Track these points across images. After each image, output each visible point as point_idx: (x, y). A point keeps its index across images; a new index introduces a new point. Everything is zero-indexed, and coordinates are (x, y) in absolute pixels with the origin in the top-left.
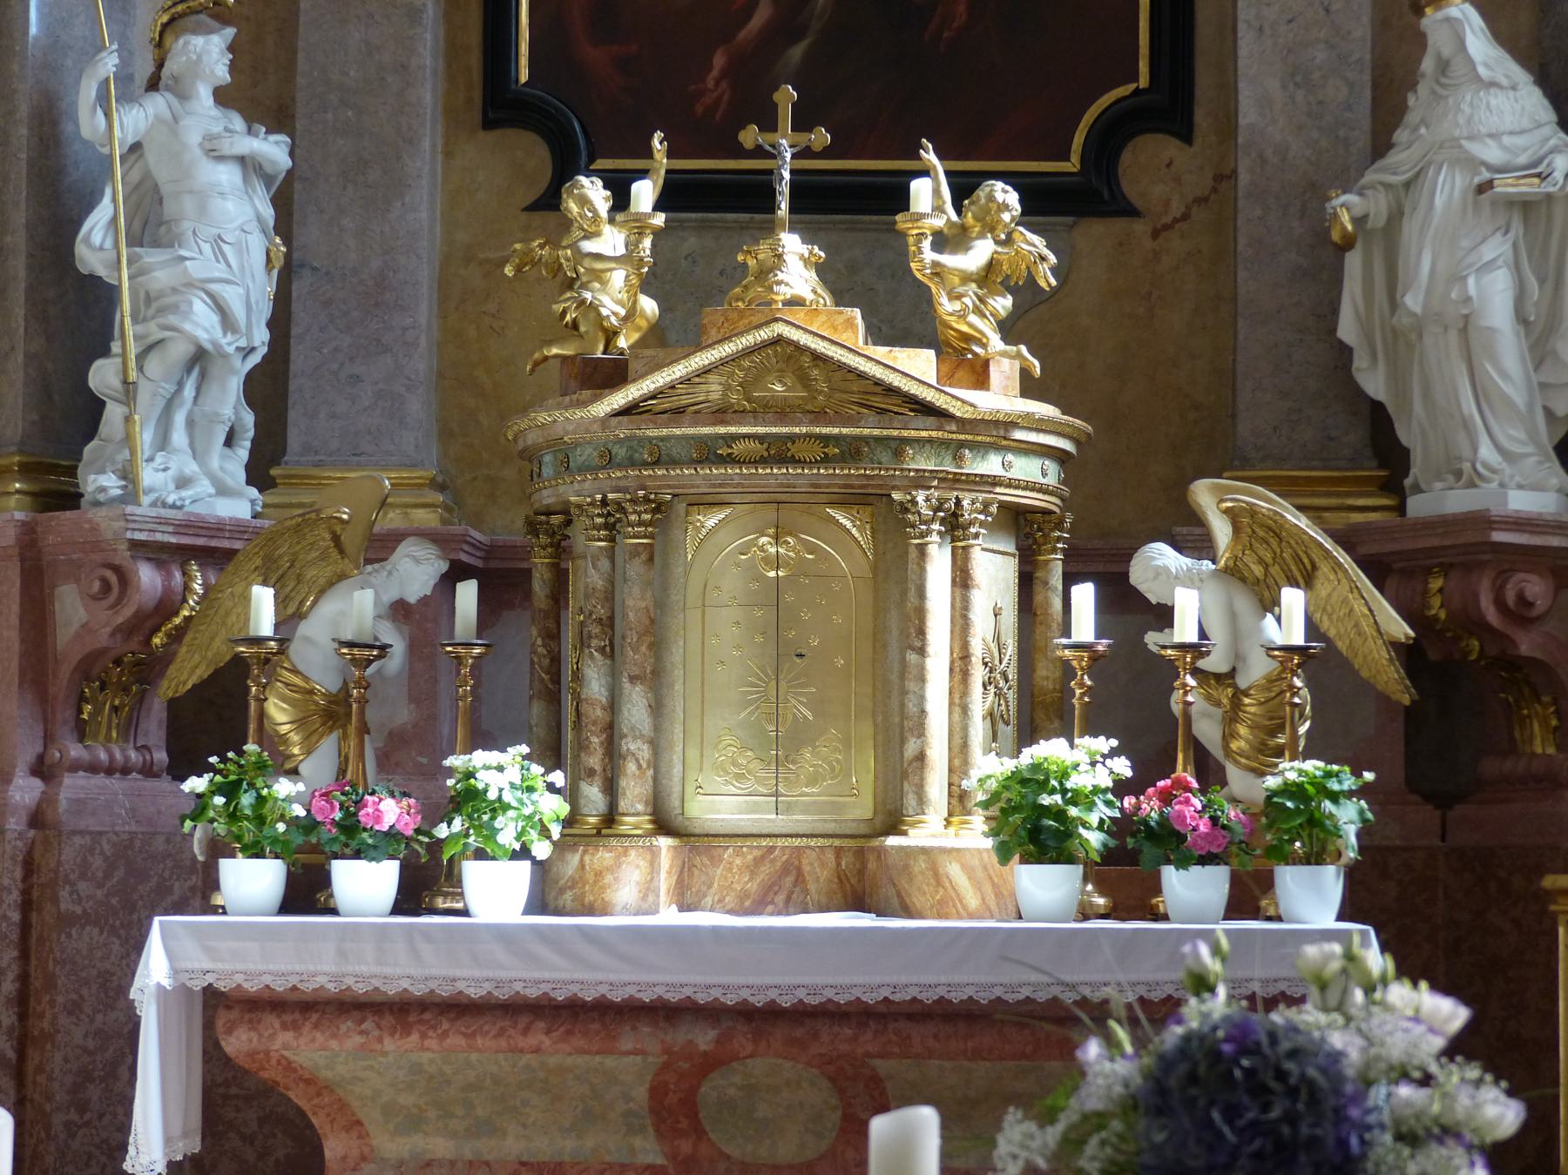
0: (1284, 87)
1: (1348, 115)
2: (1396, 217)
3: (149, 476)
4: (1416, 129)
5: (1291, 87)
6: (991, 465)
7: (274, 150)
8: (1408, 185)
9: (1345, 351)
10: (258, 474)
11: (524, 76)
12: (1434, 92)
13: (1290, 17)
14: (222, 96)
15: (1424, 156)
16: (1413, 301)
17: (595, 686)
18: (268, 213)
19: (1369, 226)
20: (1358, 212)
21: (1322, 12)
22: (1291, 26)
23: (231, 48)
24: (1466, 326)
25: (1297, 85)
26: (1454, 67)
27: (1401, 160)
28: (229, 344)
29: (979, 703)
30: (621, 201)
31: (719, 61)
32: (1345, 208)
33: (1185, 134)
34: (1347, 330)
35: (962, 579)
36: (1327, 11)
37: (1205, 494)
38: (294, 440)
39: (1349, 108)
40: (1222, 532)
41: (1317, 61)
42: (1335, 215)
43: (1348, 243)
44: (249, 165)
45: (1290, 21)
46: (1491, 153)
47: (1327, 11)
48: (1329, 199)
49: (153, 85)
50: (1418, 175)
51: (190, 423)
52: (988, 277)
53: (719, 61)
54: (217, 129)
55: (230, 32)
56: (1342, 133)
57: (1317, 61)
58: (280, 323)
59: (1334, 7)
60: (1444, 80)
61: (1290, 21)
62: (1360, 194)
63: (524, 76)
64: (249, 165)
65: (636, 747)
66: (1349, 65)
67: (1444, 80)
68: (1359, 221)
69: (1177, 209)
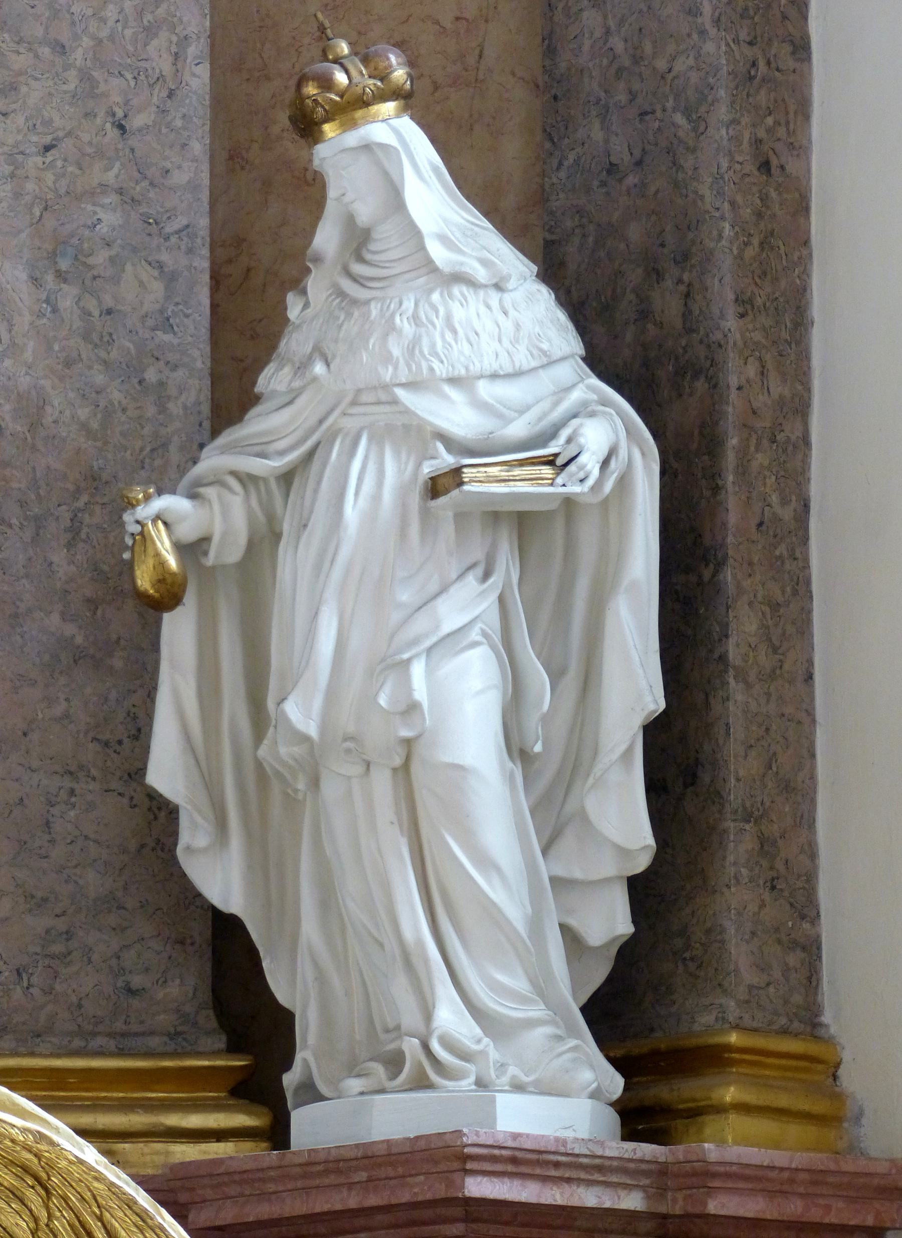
0: (36, 281)
1: (163, 337)
4: (303, 366)
5: (50, 278)
8: (287, 478)
12: (341, 294)
13: (48, 140)
15: (321, 422)
19: (210, 560)
20: (188, 532)
21: (112, 133)
22: (50, 157)
25: (61, 276)
36: (121, 127)
39: (167, 325)
41: (103, 229)
42: (144, 537)
45: (47, 148)
47: (121, 127)
48: (132, 505)
50: (310, 455)
56: (151, 375)
57: (103, 229)
59: (138, 121)
60: (358, 269)
61: (47, 148)
62: (193, 496)
66: (167, 239)
67: (358, 269)
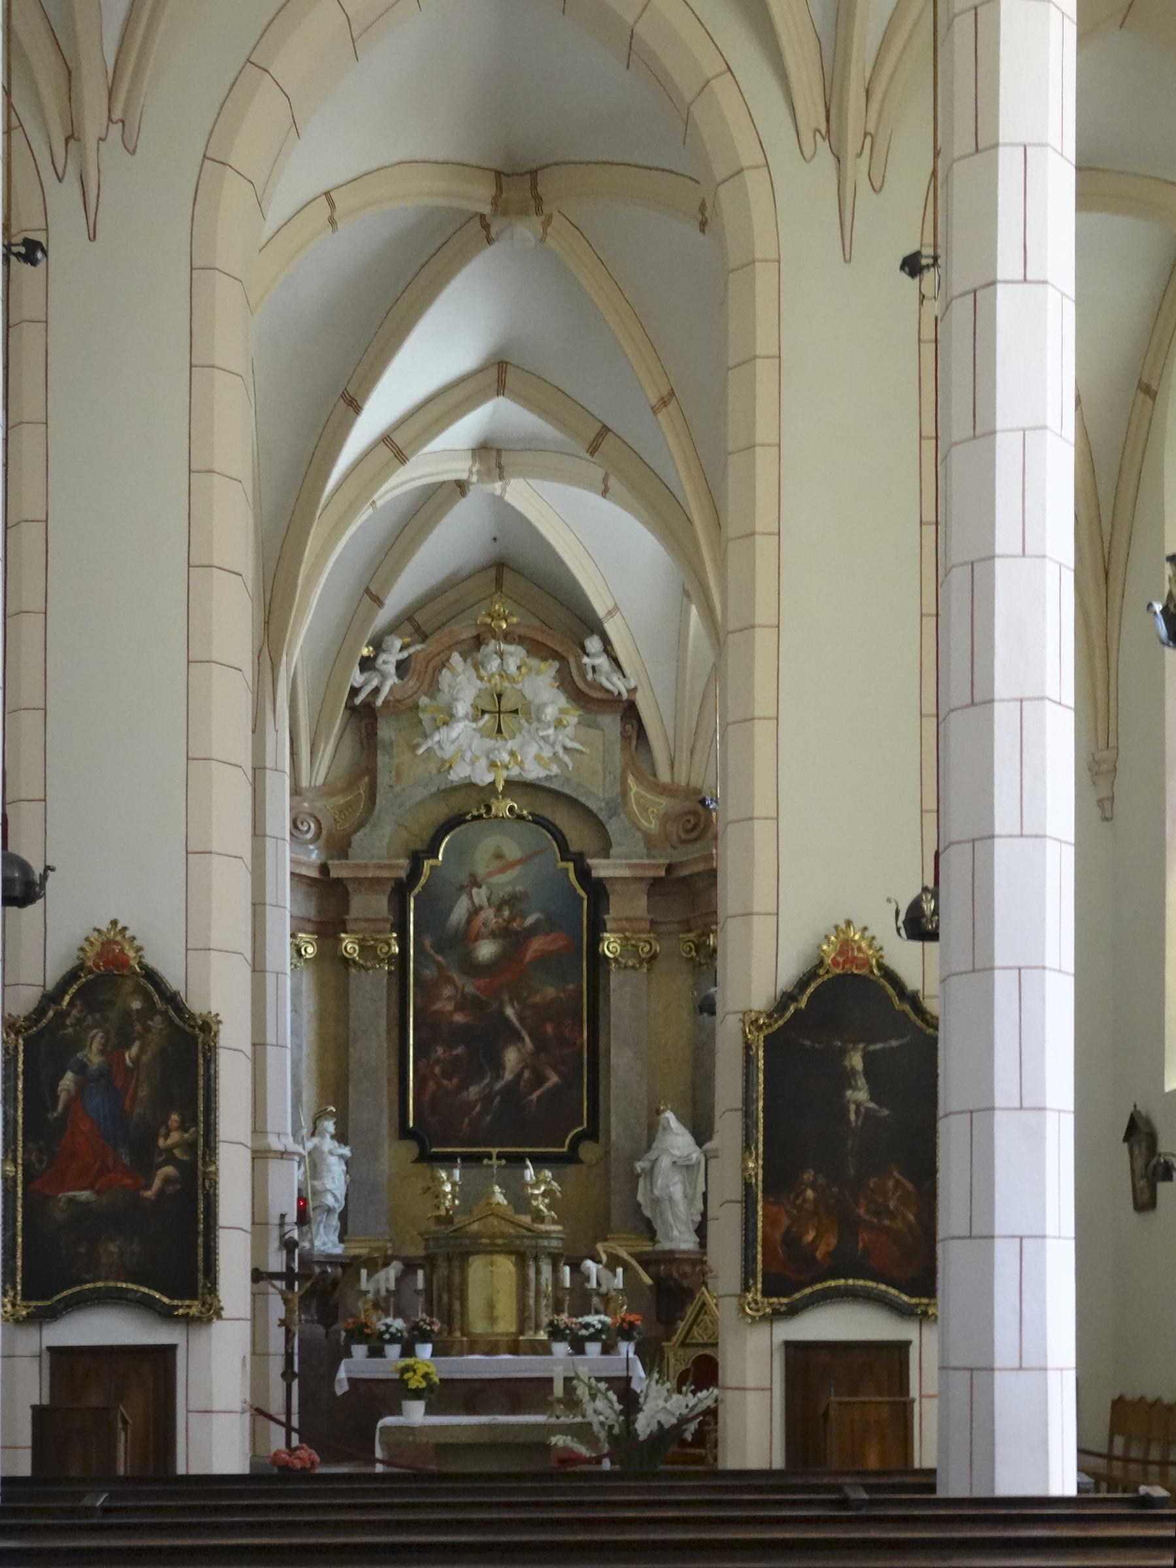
2: (652, 1168)
3: (317, 1243)
6: (546, 1243)
7: (346, 1151)
9: (639, 1205)
10: (341, 1240)
11: (411, 1124)
14: (333, 1137)
16: (656, 1192)
17: (445, 1298)
18: (344, 1168)
23: (335, 1123)
24: (671, 1199)
26: (667, 1128)
27: (652, 1155)
28: (336, 1205)
29: (544, 1302)
30: (450, 1176)
31: (466, 1120)
32: (639, 1166)
33: (597, 1141)
34: (640, 1198)
35: (538, 1272)
37: (600, 1247)
38: (349, 1230)
40: (604, 1258)
43: (639, 1176)
44: (341, 1156)
46: (677, 1153)
49: (313, 1134)
51: (325, 1227)
52: (544, 1195)
53: (466, 1120)
54: (332, 1147)
55: (335, 1120)
58: (346, 1199)
63: (411, 1124)
64: (341, 1156)
65: (457, 1317)
68: (642, 1170)
69: (594, 1162)
